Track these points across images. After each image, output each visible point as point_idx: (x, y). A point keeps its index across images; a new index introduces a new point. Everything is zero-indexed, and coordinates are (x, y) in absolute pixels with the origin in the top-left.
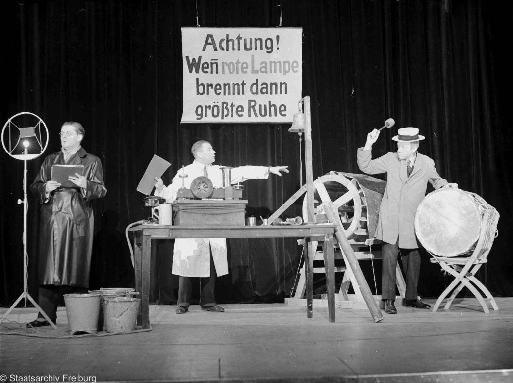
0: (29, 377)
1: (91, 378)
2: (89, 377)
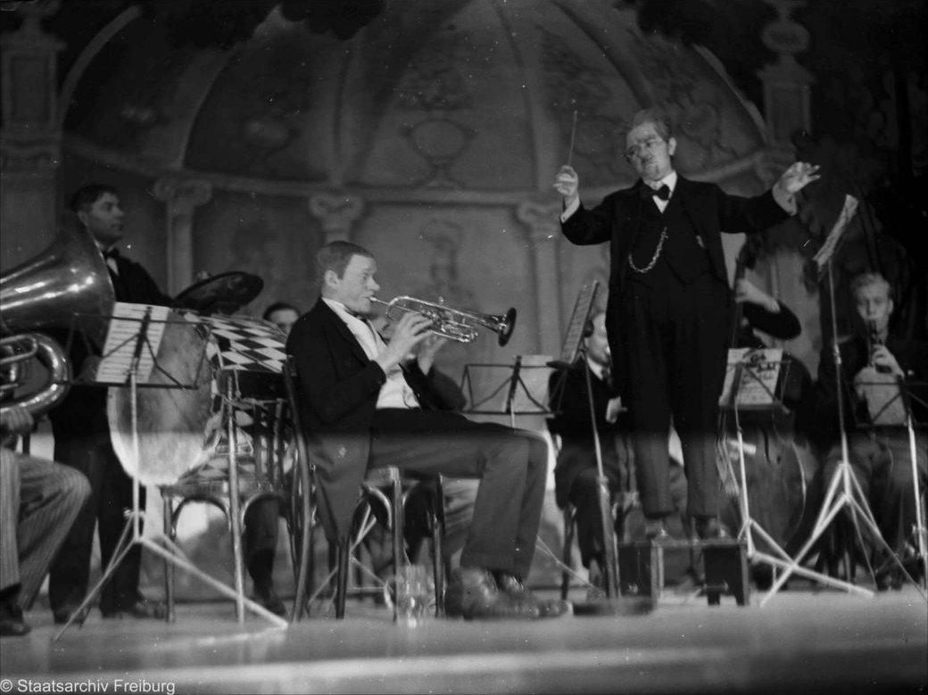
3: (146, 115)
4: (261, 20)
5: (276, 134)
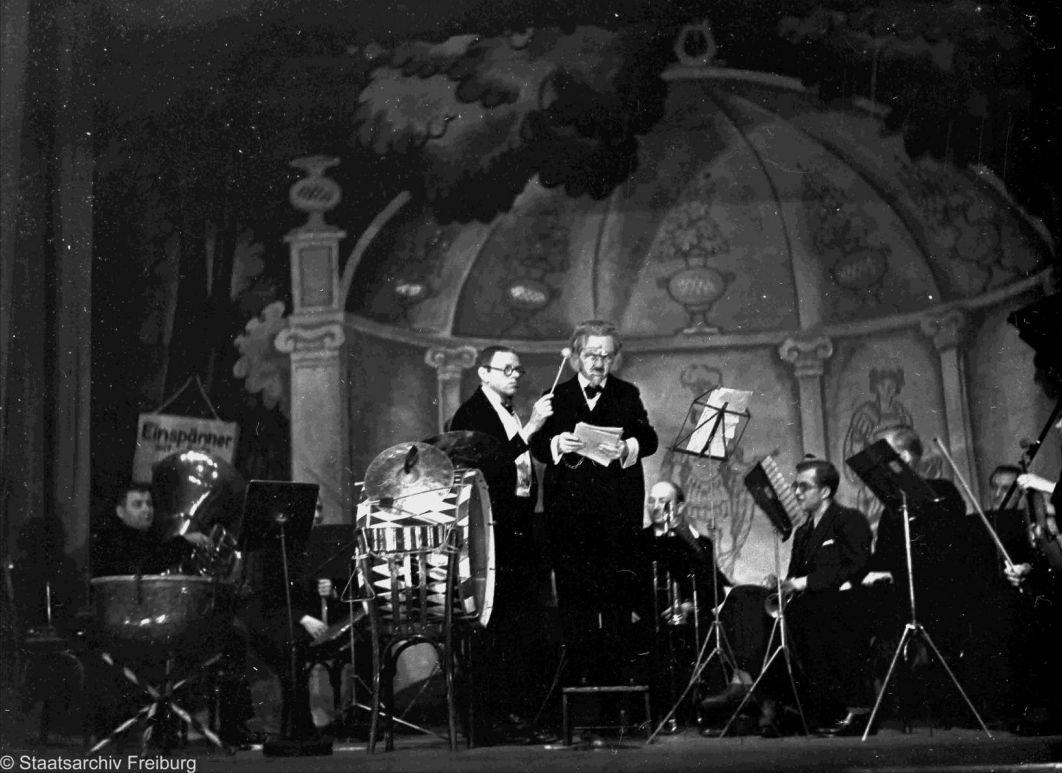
0: (60, 760)
1: (185, 763)
2: (182, 761)
3: (416, 290)
4: (519, 190)
5: (539, 297)
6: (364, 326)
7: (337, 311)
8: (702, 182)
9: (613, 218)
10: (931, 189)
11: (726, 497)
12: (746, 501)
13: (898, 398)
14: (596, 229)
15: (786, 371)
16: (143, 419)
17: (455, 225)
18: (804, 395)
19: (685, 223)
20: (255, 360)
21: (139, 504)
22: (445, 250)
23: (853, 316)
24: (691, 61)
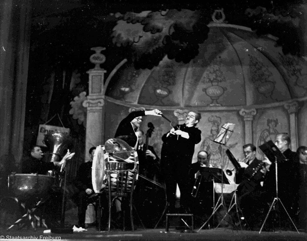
0: (19, 237)
3: (127, 89)
4: (161, 60)
5: (165, 93)
6: (111, 100)
7: (103, 95)
8: (218, 59)
9: (190, 69)
10: (290, 63)
11: (221, 157)
12: (226, 158)
13: (275, 128)
14: (186, 72)
15: (241, 118)
16: (41, 126)
17: (141, 69)
18: (246, 126)
19: (212, 71)
20: (76, 109)
21: (38, 150)
22: (137, 77)
23: (263, 103)
24: (218, 21)
